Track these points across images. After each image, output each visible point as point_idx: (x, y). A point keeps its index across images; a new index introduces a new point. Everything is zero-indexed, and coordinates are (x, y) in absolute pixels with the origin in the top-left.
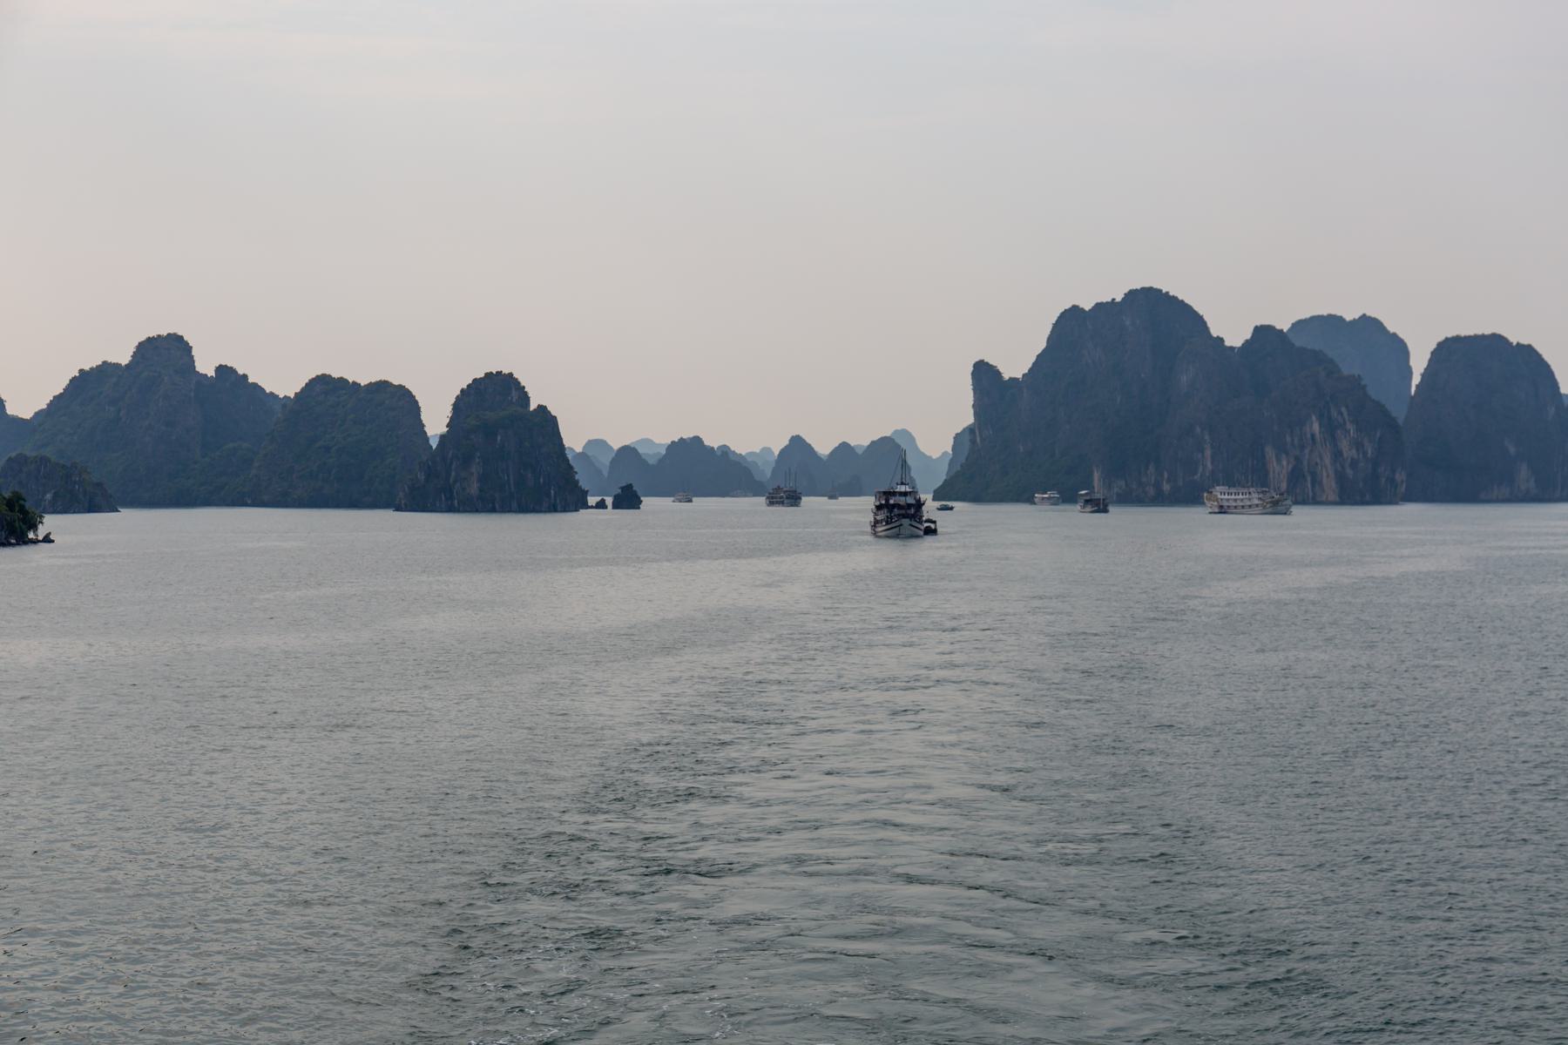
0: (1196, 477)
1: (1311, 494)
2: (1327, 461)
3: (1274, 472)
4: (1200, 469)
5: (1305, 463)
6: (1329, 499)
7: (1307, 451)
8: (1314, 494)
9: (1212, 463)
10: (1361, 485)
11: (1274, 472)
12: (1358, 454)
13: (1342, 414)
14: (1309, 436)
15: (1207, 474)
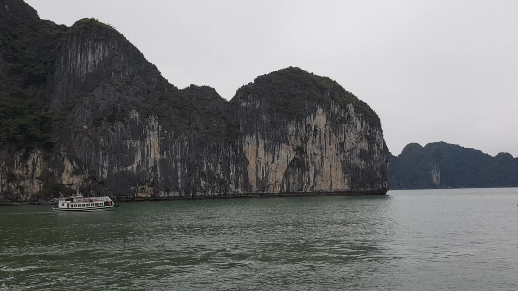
0: (129, 168)
1: (312, 184)
2: (332, 150)
3: (258, 162)
4: (138, 158)
5: (309, 153)
6: (334, 187)
7: (310, 142)
8: (315, 184)
9: (161, 153)
10: (378, 174)
11: (258, 162)
12: (370, 148)
13: (347, 110)
14: (313, 128)
15: (151, 164)
